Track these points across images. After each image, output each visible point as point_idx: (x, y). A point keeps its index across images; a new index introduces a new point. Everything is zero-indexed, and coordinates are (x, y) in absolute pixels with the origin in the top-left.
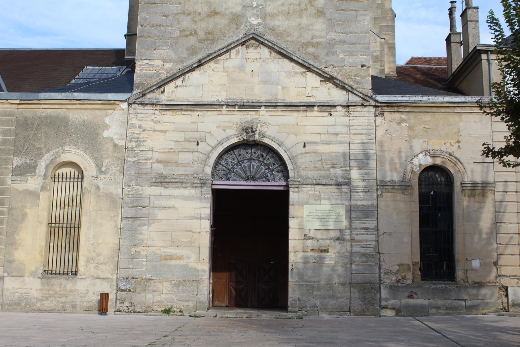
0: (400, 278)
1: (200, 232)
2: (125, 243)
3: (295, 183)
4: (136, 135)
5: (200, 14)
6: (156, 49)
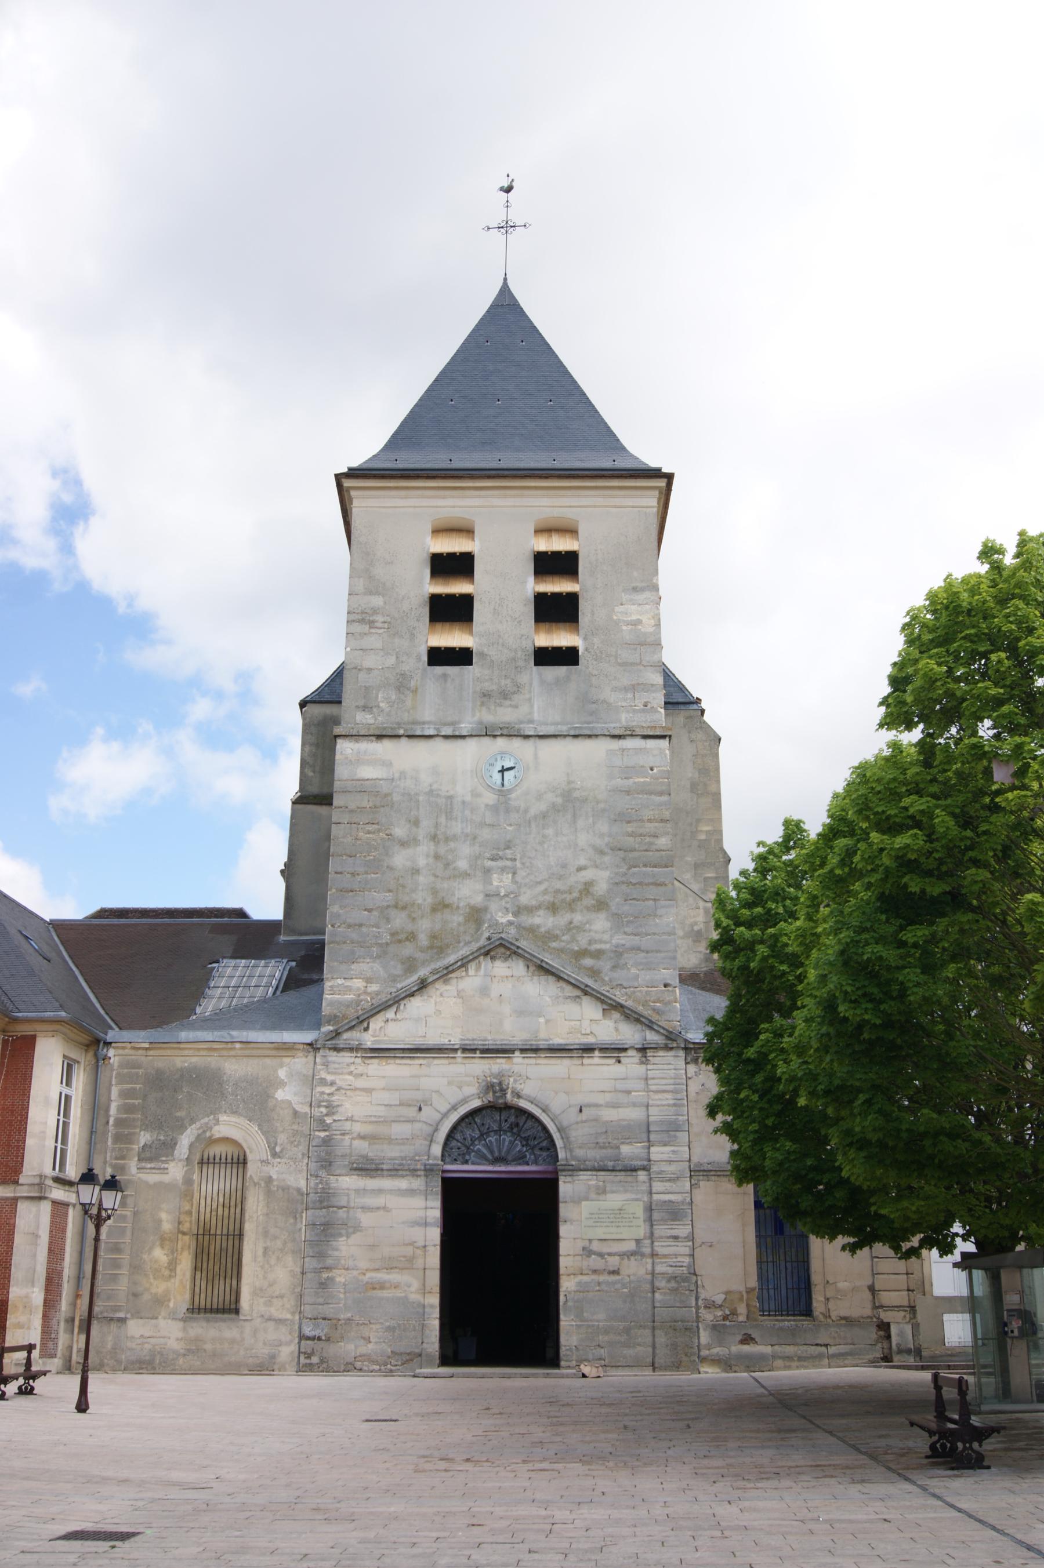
3: (567, 1167)
4: (326, 1097)
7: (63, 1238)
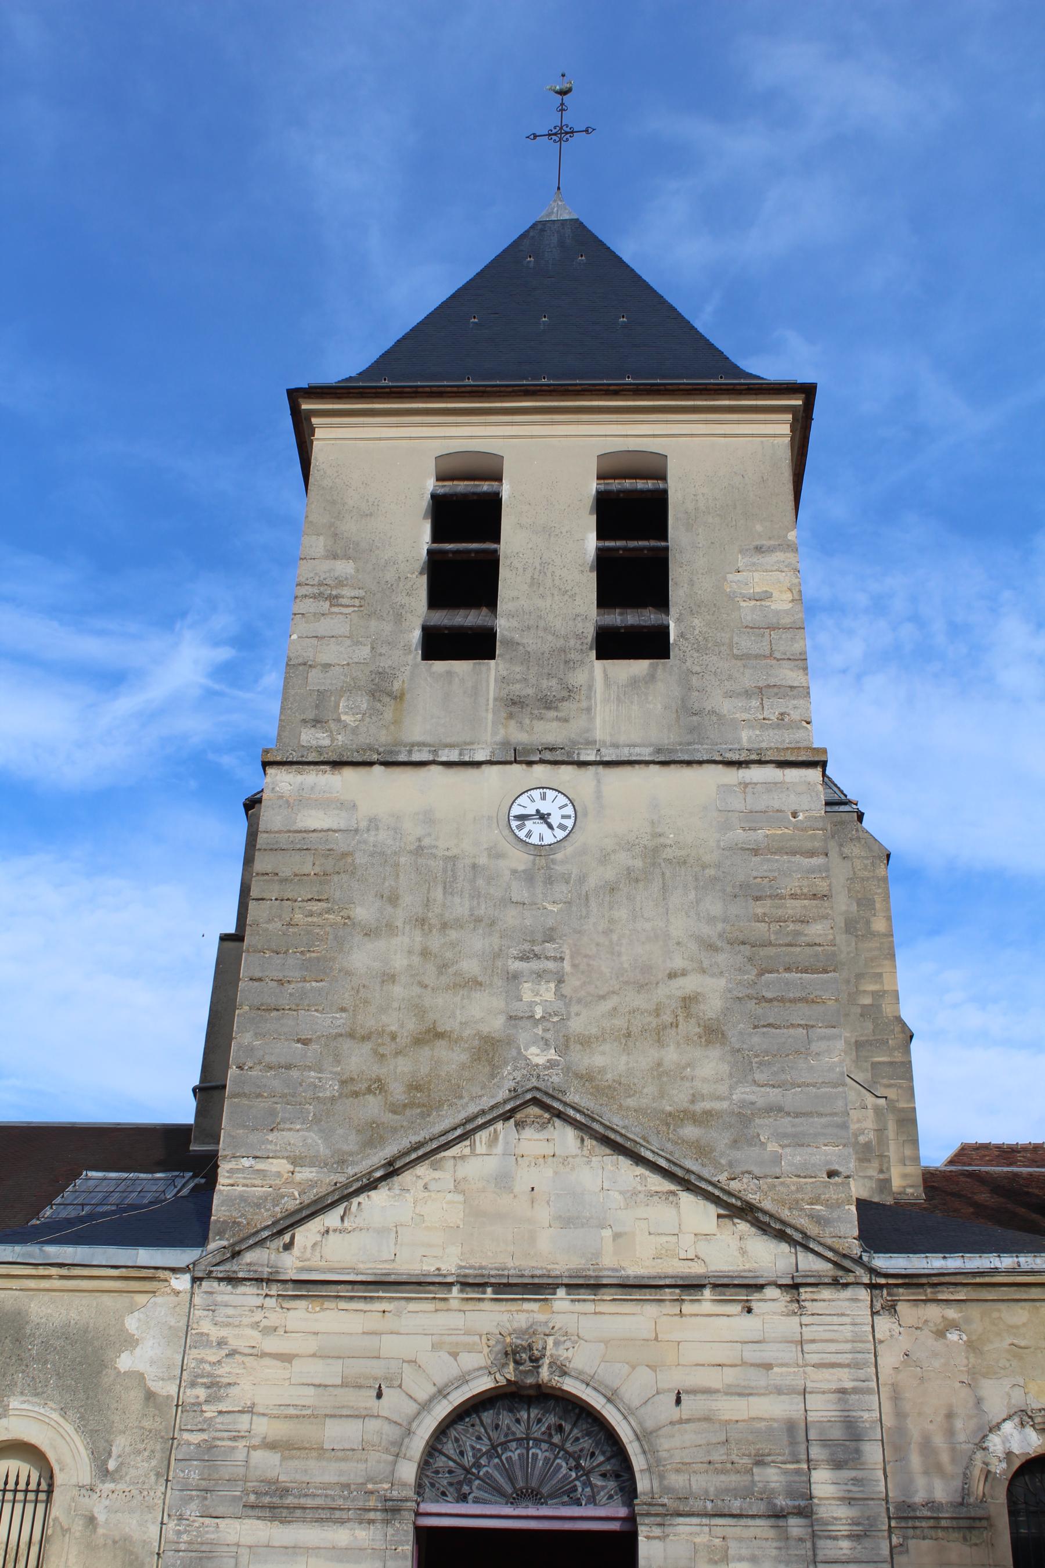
4: (208, 1368)
5: (394, 1037)
6: (275, 1130)
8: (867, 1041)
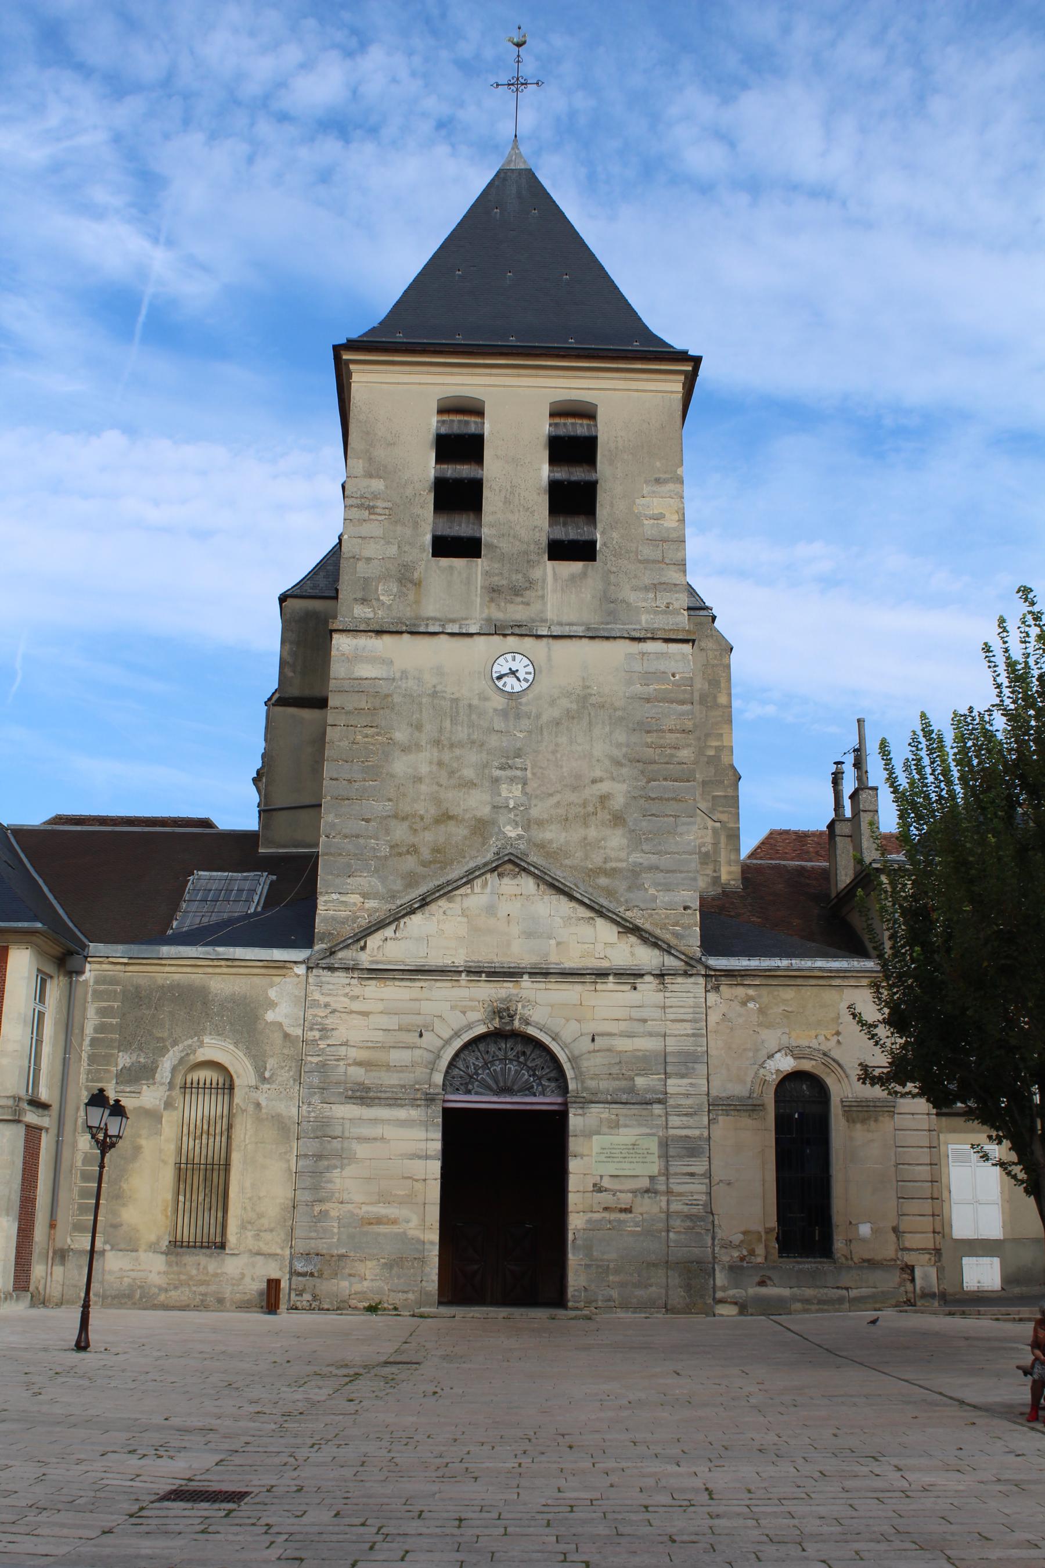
0: (745, 1253)
1: (425, 1180)
2: (304, 1196)
4: (320, 1020)
5: (422, 818)
7: (37, 1165)
8: (710, 781)
